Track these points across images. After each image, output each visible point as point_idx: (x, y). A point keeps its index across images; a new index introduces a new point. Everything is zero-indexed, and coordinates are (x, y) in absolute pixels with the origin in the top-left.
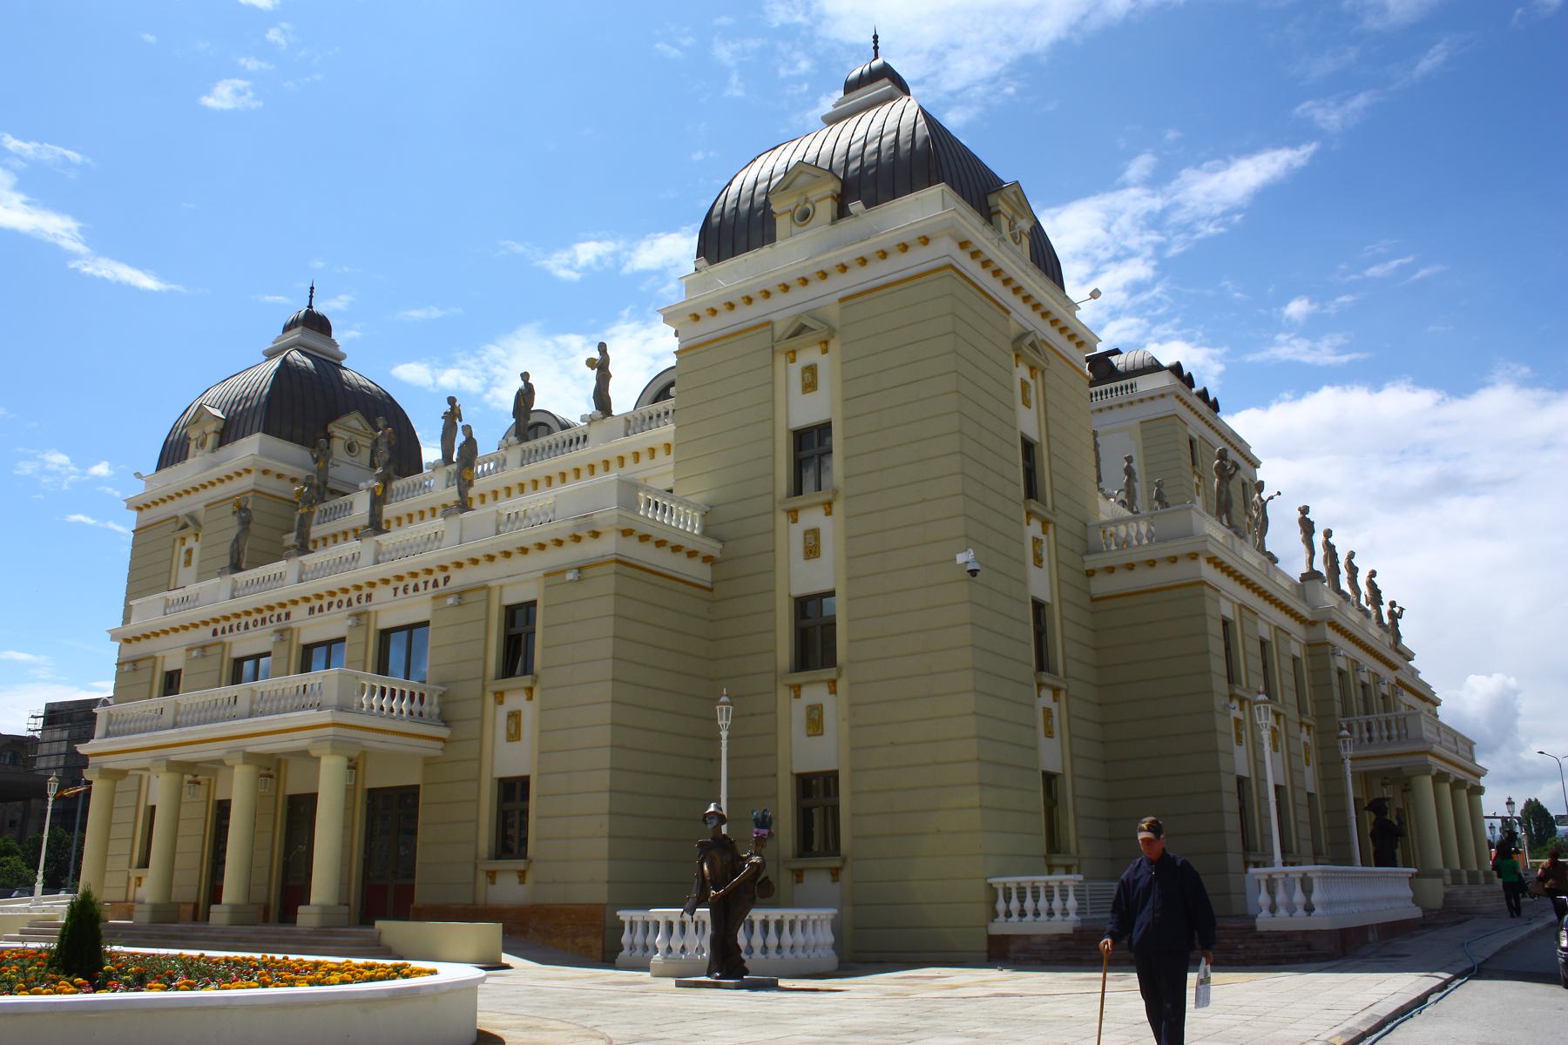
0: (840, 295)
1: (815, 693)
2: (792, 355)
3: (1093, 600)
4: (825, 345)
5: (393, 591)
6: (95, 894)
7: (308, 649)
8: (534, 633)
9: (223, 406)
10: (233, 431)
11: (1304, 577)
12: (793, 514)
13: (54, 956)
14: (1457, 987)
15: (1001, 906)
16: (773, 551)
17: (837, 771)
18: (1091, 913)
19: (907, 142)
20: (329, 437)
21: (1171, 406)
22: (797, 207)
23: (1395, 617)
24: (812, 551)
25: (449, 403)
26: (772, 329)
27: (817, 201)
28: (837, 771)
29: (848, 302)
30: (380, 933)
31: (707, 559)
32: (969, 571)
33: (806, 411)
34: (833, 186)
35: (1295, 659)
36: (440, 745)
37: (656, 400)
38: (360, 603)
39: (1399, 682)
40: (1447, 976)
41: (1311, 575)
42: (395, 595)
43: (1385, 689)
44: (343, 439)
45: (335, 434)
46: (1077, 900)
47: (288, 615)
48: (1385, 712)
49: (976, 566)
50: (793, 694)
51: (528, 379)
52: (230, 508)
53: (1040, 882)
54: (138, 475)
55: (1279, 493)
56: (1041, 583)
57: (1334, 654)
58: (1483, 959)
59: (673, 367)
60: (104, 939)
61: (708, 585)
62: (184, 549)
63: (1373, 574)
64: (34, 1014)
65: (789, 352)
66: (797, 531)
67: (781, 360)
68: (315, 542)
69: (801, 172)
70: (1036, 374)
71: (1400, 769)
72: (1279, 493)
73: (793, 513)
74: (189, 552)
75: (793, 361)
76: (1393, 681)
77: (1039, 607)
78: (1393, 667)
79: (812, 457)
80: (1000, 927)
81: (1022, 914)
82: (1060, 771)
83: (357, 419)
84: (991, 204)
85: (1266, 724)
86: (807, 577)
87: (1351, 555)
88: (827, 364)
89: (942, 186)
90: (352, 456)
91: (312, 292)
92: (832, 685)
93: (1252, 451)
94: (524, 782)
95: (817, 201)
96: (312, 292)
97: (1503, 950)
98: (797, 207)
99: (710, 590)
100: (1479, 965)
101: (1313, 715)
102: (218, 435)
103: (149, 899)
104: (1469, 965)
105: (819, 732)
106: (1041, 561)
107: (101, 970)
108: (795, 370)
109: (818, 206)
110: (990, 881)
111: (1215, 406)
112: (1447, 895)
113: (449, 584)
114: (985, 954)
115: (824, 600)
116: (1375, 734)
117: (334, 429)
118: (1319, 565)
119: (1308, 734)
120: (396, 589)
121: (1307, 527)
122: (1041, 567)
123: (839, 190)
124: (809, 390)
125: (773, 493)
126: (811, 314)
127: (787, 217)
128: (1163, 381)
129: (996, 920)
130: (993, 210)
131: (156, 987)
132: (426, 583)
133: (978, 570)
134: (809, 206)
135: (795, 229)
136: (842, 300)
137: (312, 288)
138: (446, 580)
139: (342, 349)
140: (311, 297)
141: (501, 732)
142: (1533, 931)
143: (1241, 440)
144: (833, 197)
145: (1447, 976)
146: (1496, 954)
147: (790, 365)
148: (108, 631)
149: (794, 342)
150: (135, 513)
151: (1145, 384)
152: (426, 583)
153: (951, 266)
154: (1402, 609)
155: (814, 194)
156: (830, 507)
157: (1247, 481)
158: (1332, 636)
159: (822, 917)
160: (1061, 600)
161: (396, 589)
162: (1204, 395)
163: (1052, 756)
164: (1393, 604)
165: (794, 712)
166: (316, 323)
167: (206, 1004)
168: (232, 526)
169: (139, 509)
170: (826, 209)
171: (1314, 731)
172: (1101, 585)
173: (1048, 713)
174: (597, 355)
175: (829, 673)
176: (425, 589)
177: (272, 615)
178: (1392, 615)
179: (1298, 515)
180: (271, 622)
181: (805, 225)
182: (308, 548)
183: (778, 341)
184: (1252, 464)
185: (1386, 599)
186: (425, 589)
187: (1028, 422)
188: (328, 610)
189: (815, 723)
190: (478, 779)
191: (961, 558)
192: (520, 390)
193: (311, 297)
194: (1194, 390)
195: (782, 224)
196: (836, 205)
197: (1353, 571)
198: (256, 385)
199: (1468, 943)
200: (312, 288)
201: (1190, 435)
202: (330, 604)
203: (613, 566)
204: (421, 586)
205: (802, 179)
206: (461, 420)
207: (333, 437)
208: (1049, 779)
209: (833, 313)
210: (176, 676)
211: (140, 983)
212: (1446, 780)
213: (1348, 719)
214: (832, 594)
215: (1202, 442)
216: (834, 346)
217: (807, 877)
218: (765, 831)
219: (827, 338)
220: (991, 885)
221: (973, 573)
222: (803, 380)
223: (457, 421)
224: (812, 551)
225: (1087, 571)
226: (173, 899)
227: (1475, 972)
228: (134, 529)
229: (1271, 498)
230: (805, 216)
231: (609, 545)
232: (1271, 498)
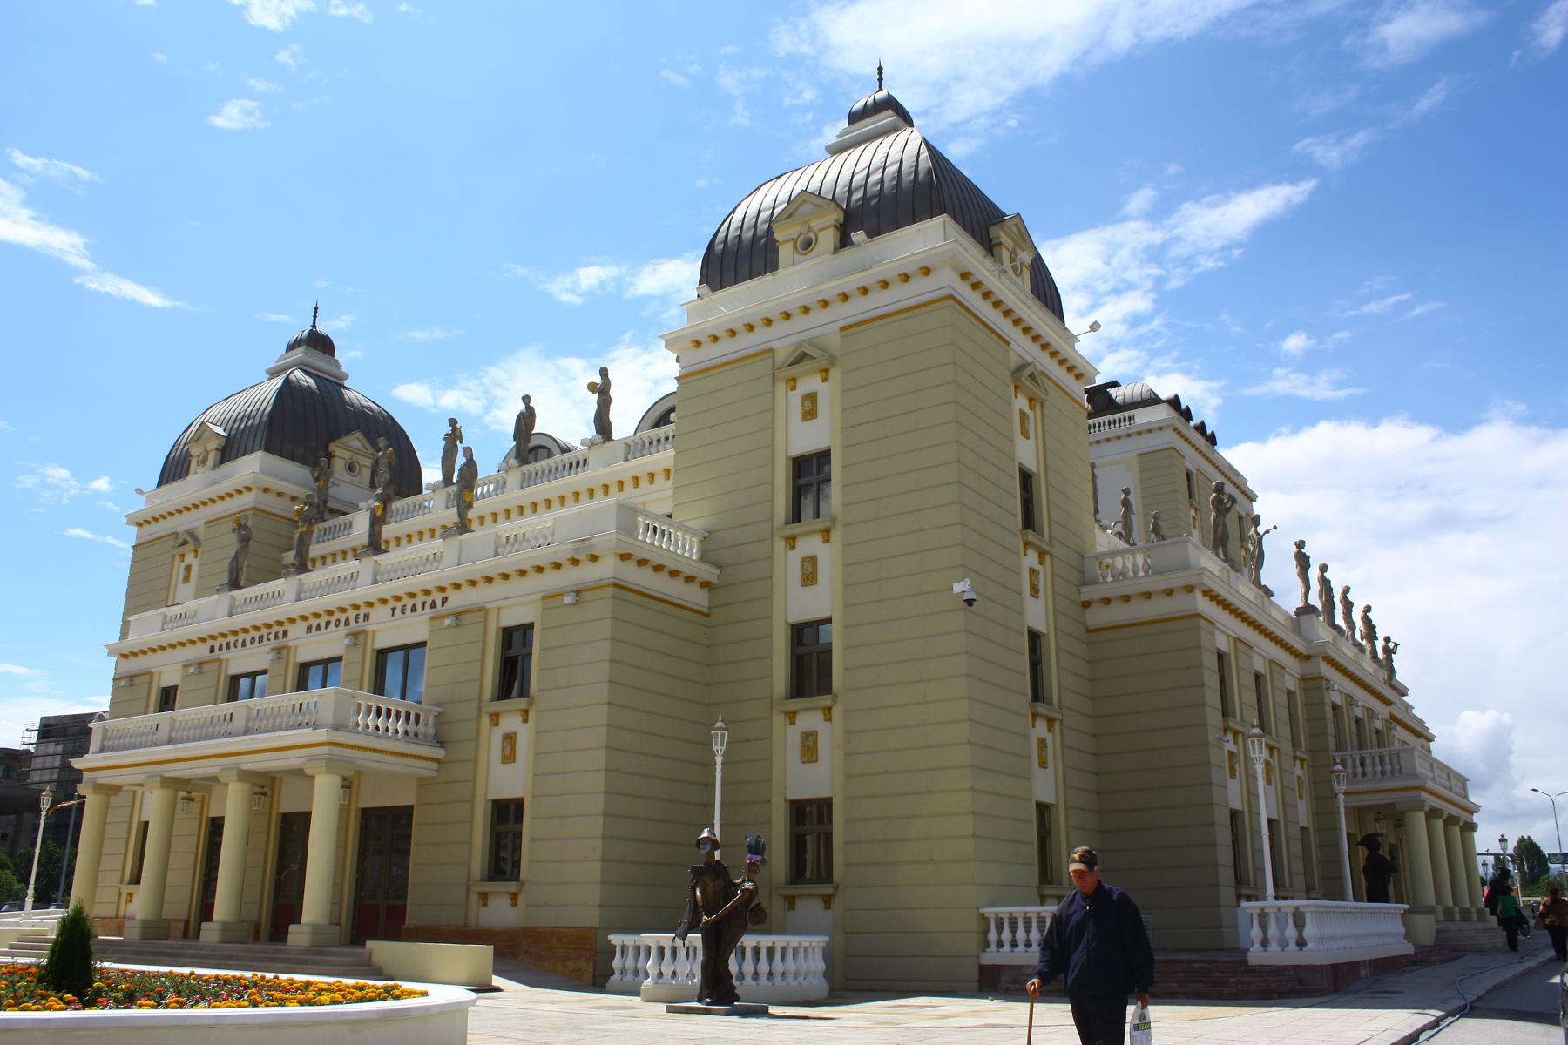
0: (842, 323)
1: (811, 720)
2: (792, 382)
3: (1089, 631)
4: (825, 373)
5: (391, 612)
6: (87, 910)
7: (304, 668)
8: (530, 655)
9: (224, 425)
10: (234, 450)
11: (1299, 612)
12: (791, 541)
13: (43, 971)
14: (1449, 1025)
15: (993, 936)
16: (771, 577)
17: (831, 799)
19: (911, 173)
20: (330, 456)
21: (1169, 439)
22: (798, 237)
23: (1389, 652)
24: (809, 578)
26: (773, 357)
28: (831, 799)
30: (371, 953)
31: (705, 585)
32: (965, 601)
33: (806, 438)
34: (836, 216)
35: (1289, 693)
36: (434, 765)
37: (656, 425)
38: (357, 622)
39: (1393, 717)
40: (1439, 1013)
41: (1307, 610)
42: (393, 615)
43: (1378, 724)
45: (337, 453)
47: (285, 634)
48: (1379, 747)
49: (973, 596)
50: (788, 721)
51: (529, 402)
52: (230, 525)
53: (1033, 912)
54: (139, 491)
55: (1275, 528)
56: (1037, 614)
57: (1328, 689)
58: (1476, 997)
59: (674, 393)
60: (95, 955)
61: (706, 611)
62: (183, 565)
63: (1368, 609)
64: (23, 1031)
66: (795, 558)
67: (781, 387)
68: (314, 561)
69: (804, 201)
70: (1035, 405)
71: (1393, 804)
72: (1275, 528)
73: (791, 541)
74: (188, 568)
75: (794, 388)
76: (1388, 717)
77: (1034, 637)
78: (1387, 702)
79: (811, 485)
80: (991, 957)
81: (1014, 944)
82: (1053, 802)
83: (358, 438)
84: (992, 236)
85: (1260, 758)
87: (1347, 590)
88: (827, 392)
89: (944, 218)
91: (316, 312)
93: (1249, 485)
94: (518, 804)
96: (316, 312)
97: (1495, 987)
98: (801, 234)
99: (708, 615)
100: (1471, 1003)
101: (1306, 750)
102: (219, 453)
103: (138, 916)
104: (1462, 1003)
105: (814, 759)
106: (1037, 592)
107: (91, 986)
108: (796, 398)
109: (820, 235)
110: (982, 910)
111: (1212, 440)
112: (1439, 932)
113: (446, 606)
115: (821, 627)
116: (1369, 769)
117: (335, 448)
118: (1315, 600)
119: (1302, 768)
120: (394, 609)
121: (1303, 561)
122: (1037, 598)
123: (842, 220)
124: (809, 417)
126: (811, 342)
127: (790, 246)
128: (1161, 413)
129: (987, 950)
130: (994, 242)
131: (146, 1005)
133: (975, 600)
134: (812, 235)
135: (798, 257)
136: (843, 329)
137: (316, 308)
138: (444, 601)
139: (344, 369)
140: (315, 317)
141: (496, 754)
142: (1525, 970)
143: (1238, 474)
144: (835, 227)
145: (1439, 1013)
146: (1488, 992)
147: (791, 393)
149: (795, 370)
150: (135, 529)
151: (1143, 417)
153: (952, 297)
154: (1396, 645)
155: (816, 224)
156: (828, 535)
157: (1244, 514)
158: (1326, 670)
159: (814, 945)
160: (1056, 630)
161: (394, 609)
162: (1201, 428)
163: (1045, 787)
164: (1387, 639)
165: (788, 738)
166: (319, 343)
167: (195, 1023)
168: (231, 544)
169: (139, 525)
170: (828, 238)
172: (1098, 616)
173: (1042, 743)
174: (598, 380)
175: (825, 700)
176: (423, 609)
177: (270, 633)
178: (1387, 651)
179: (1295, 549)
180: (269, 640)
181: (805, 254)
182: (306, 566)
183: (778, 369)
184: (1249, 498)
185: (1381, 634)
186: (423, 609)
187: (1027, 453)
188: (326, 628)
189: (809, 749)
190: (472, 800)
191: (958, 588)
192: (521, 413)
193: (315, 317)
194: (1192, 423)
195: (785, 252)
196: (838, 234)
197: (1348, 605)
198: (259, 404)
199: (1460, 981)
200: (316, 308)
201: (1187, 468)
202: (328, 624)
203: (611, 590)
204: (419, 607)
205: (805, 208)
206: (461, 442)
207: (334, 456)
208: (1043, 809)
209: (834, 341)
210: (172, 694)
211: (129, 1000)
213: (1340, 753)
214: (828, 621)
215: (1201, 476)
216: (835, 374)
218: (759, 858)
219: (827, 367)
220: (983, 915)
221: (970, 602)
223: (458, 443)
224: (809, 578)
225: (1083, 603)
226: (164, 917)
227: (1467, 1009)
228: (134, 544)
229: (1267, 532)
230: (808, 245)
231: (606, 569)
232: (1267, 532)
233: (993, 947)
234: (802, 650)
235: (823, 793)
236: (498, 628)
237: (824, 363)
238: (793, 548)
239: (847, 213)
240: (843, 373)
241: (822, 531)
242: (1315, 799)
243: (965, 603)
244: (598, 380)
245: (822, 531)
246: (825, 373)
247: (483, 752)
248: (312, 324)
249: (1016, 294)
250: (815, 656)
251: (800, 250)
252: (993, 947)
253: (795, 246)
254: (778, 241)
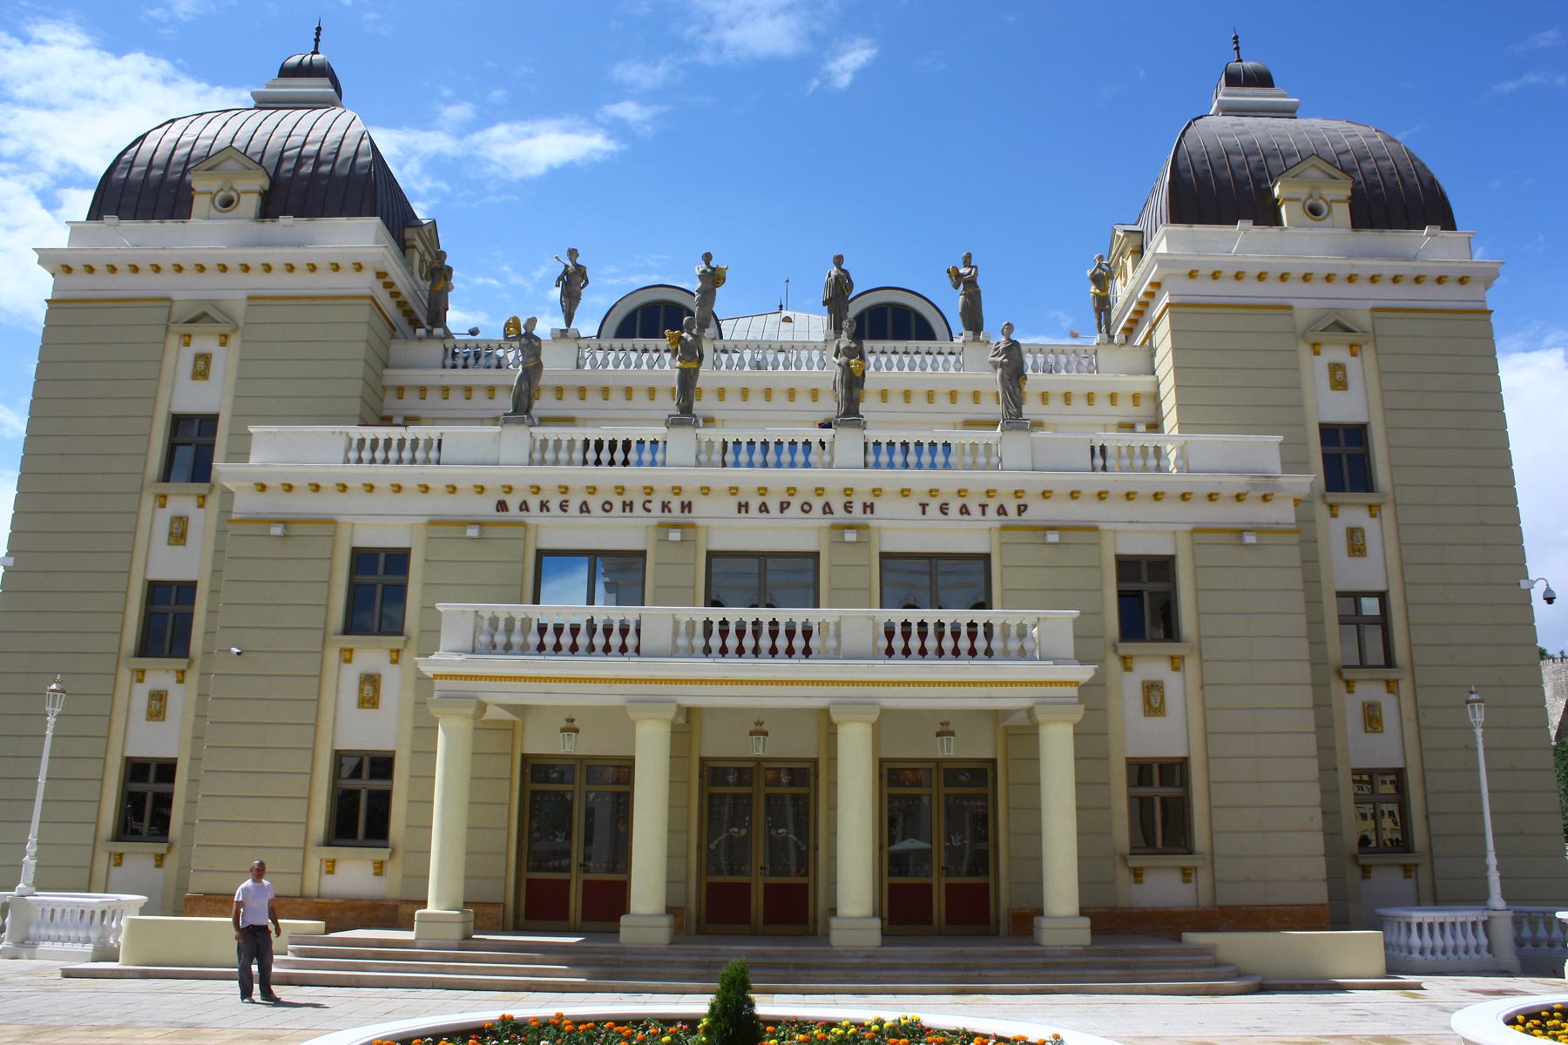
0: (251, 293)
2: (187, 339)
4: (224, 340)
12: (162, 500)
19: (331, 153)
22: (219, 192)
26: (170, 307)
27: (243, 192)
34: (261, 182)
65: (185, 335)
66: (164, 516)
67: (174, 342)
69: (231, 157)
73: (162, 499)
75: (187, 344)
84: (406, 236)
88: (225, 361)
89: (377, 220)
92: (181, 676)
95: (243, 192)
98: (222, 190)
108: (188, 355)
109: (243, 197)
123: (267, 187)
125: (143, 474)
126: (213, 303)
127: (208, 197)
130: (408, 243)
134: (233, 194)
135: (213, 211)
144: (260, 194)
149: (189, 328)
153: (372, 299)
155: (241, 185)
156: (204, 500)
170: (250, 203)
181: (224, 212)
183: (175, 323)
195: (200, 204)
196: (260, 199)
205: (231, 165)
209: (239, 310)
216: (234, 341)
217: (1374, 873)
219: (227, 333)
222: (195, 365)
230: (228, 203)
237: (226, 329)
238: (163, 506)
239: (275, 180)
240: (243, 341)
241: (199, 496)
245: (199, 496)
246: (224, 340)
250: (171, 615)
251: (218, 205)
253: (213, 201)
254: (194, 190)
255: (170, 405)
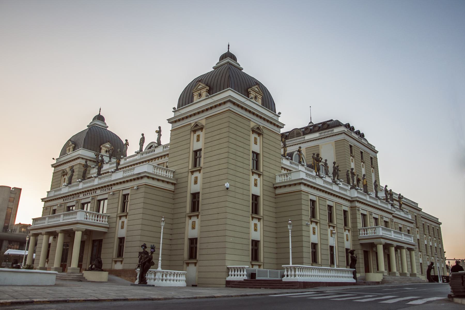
1: (194, 219)
5: (100, 191)
10: (76, 148)
16: (187, 182)
18: (269, 277)
20: (101, 149)
21: (343, 137)
24: (196, 182)
25: (126, 141)
29: (207, 119)
31: (172, 184)
32: (226, 188)
33: (197, 146)
36: (107, 229)
42: (101, 192)
44: (104, 150)
46: (246, 271)
50: (189, 218)
51: (143, 135)
54: (53, 159)
61: (173, 190)
62: (64, 178)
74: (65, 179)
80: (229, 278)
83: (108, 144)
84: (249, 91)
86: (195, 188)
90: (107, 154)
99: (174, 192)
101: (351, 227)
105: (194, 228)
109: (203, 93)
110: (228, 267)
111: (362, 136)
112: (383, 278)
114: (225, 285)
117: (102, 147)
120: (101, 190)
122: (257, 187)
128: (342, 129)
132: (107, 189)
133: (229, 188)
136: (206, 118)
138: (111, 188)
148: (41, 199)
151: (336, 130)
152: (107, 189)
158: (357, 204)
159: (181, 273)
162: (358, 133)
163: (256, 236)
165: (189, 222)
166: (100, 118)
169: (55, 167)
171: (351, 231)
174: (158, 130)
176: (107, 190)
180: (75, 198)
186: (107, 190)
187: (256, 148)
192: (141, 138)
201: (350, 145)
202: (88, 194)
203: (145, 186)
204: (106, 189)
206: (128, 146)
207: (102, 149)
212: (393, 247)
213: (366, 227)
221: (227, 188)
223: (128, 146)
224: (196, 182)
228: (53, 172)
233: (230, 276)
234: (195, 200)
235: (196, 237)
236: (122, 194)
242: (353, 241)
243: (226, 189)
244: (158, 130)
247: (117, 225)
248: (99, 113)
249: (256, 106)
252: (230, 276)
255: (193, 149)
